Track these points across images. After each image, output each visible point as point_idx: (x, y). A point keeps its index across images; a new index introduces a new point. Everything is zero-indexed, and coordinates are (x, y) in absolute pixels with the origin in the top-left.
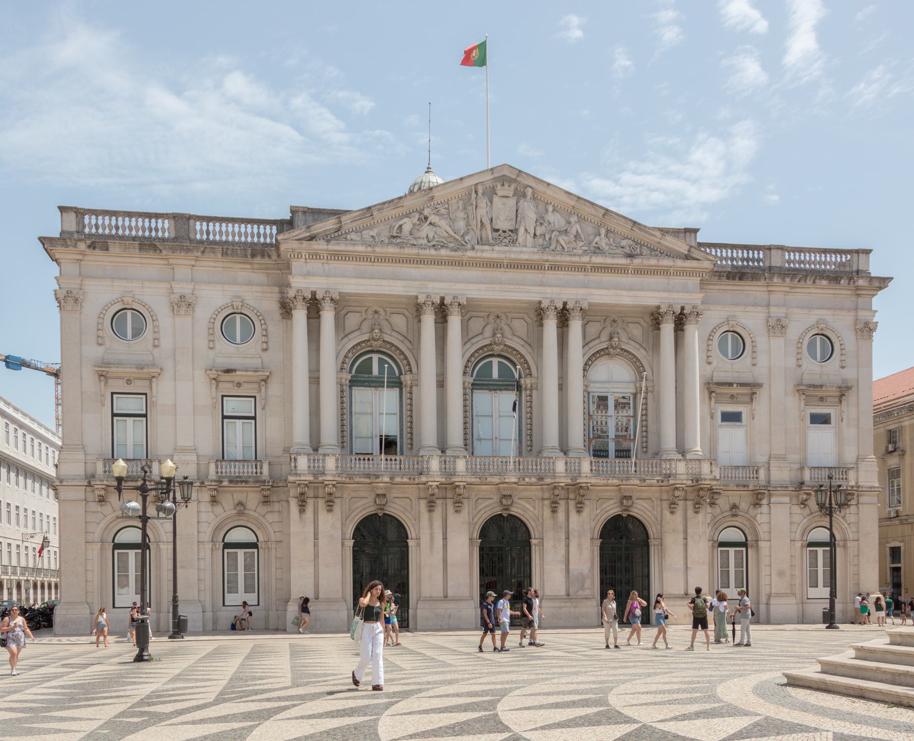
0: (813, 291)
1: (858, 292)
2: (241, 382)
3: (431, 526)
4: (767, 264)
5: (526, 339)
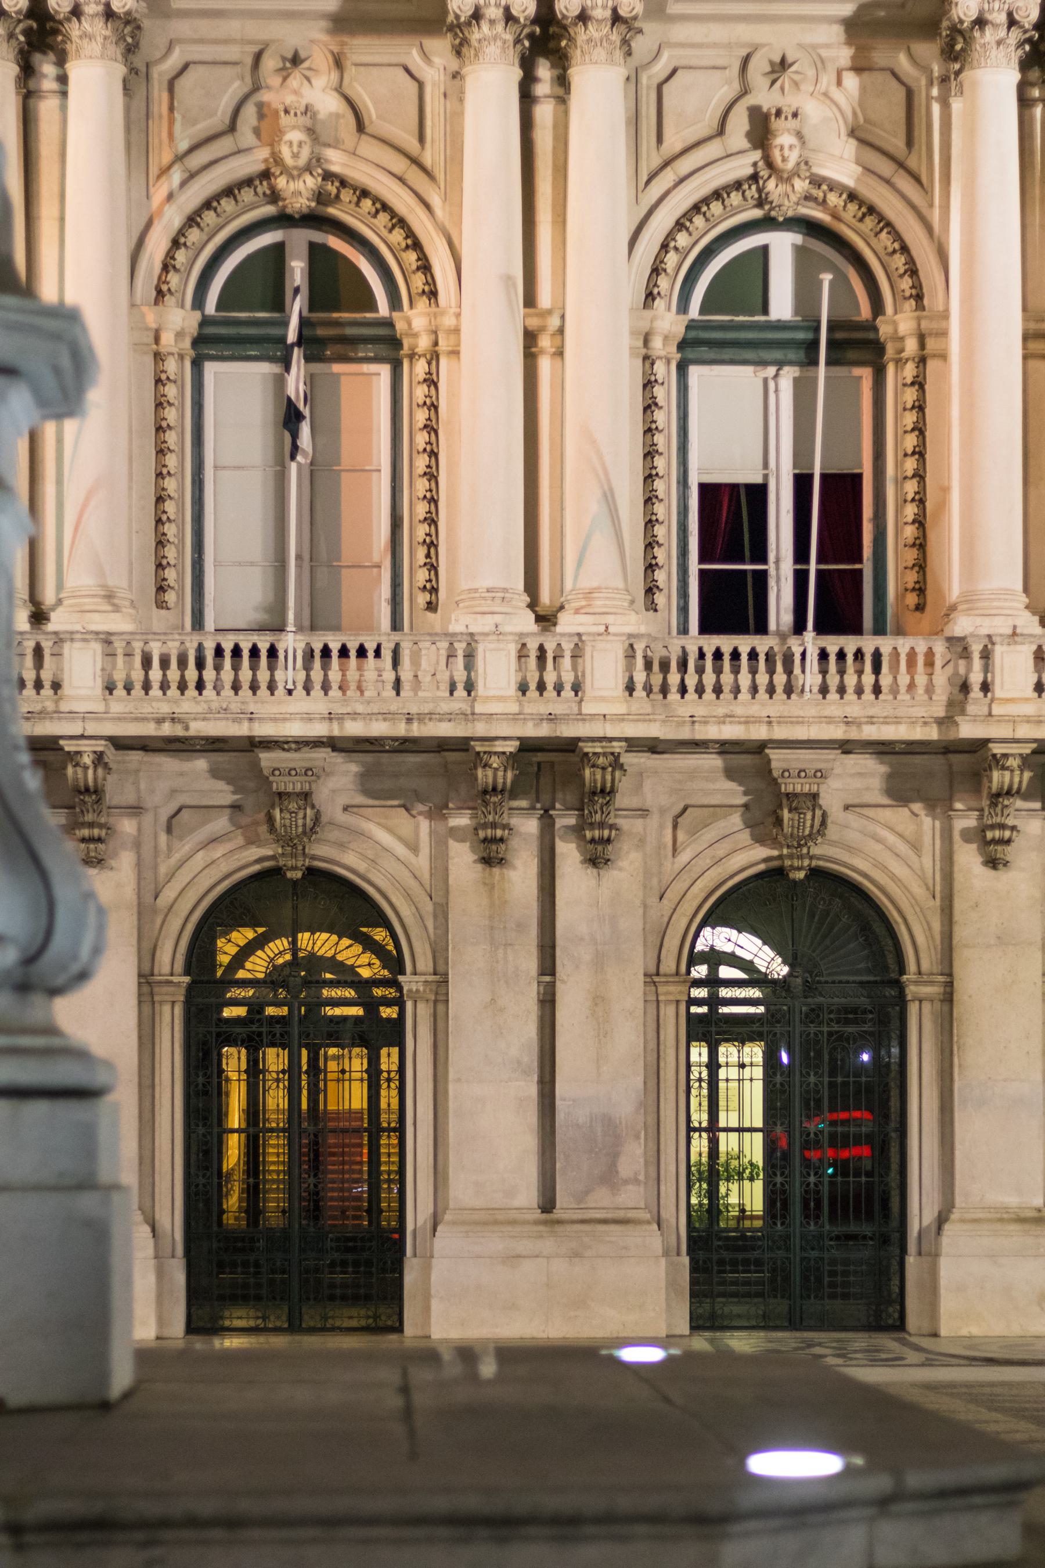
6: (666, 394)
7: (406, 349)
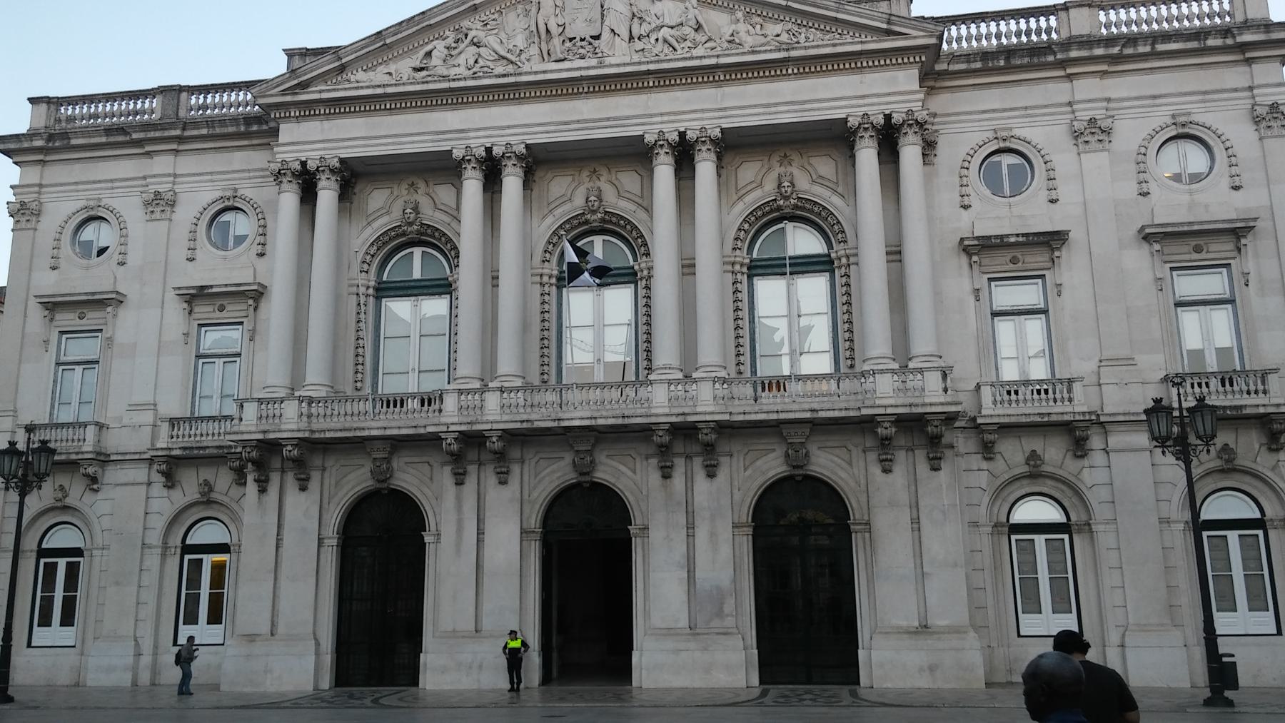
1: (1248, 55)
4: (1064, 34)
5: (640, 201)
6: (744, 287)
7: (639, 277)
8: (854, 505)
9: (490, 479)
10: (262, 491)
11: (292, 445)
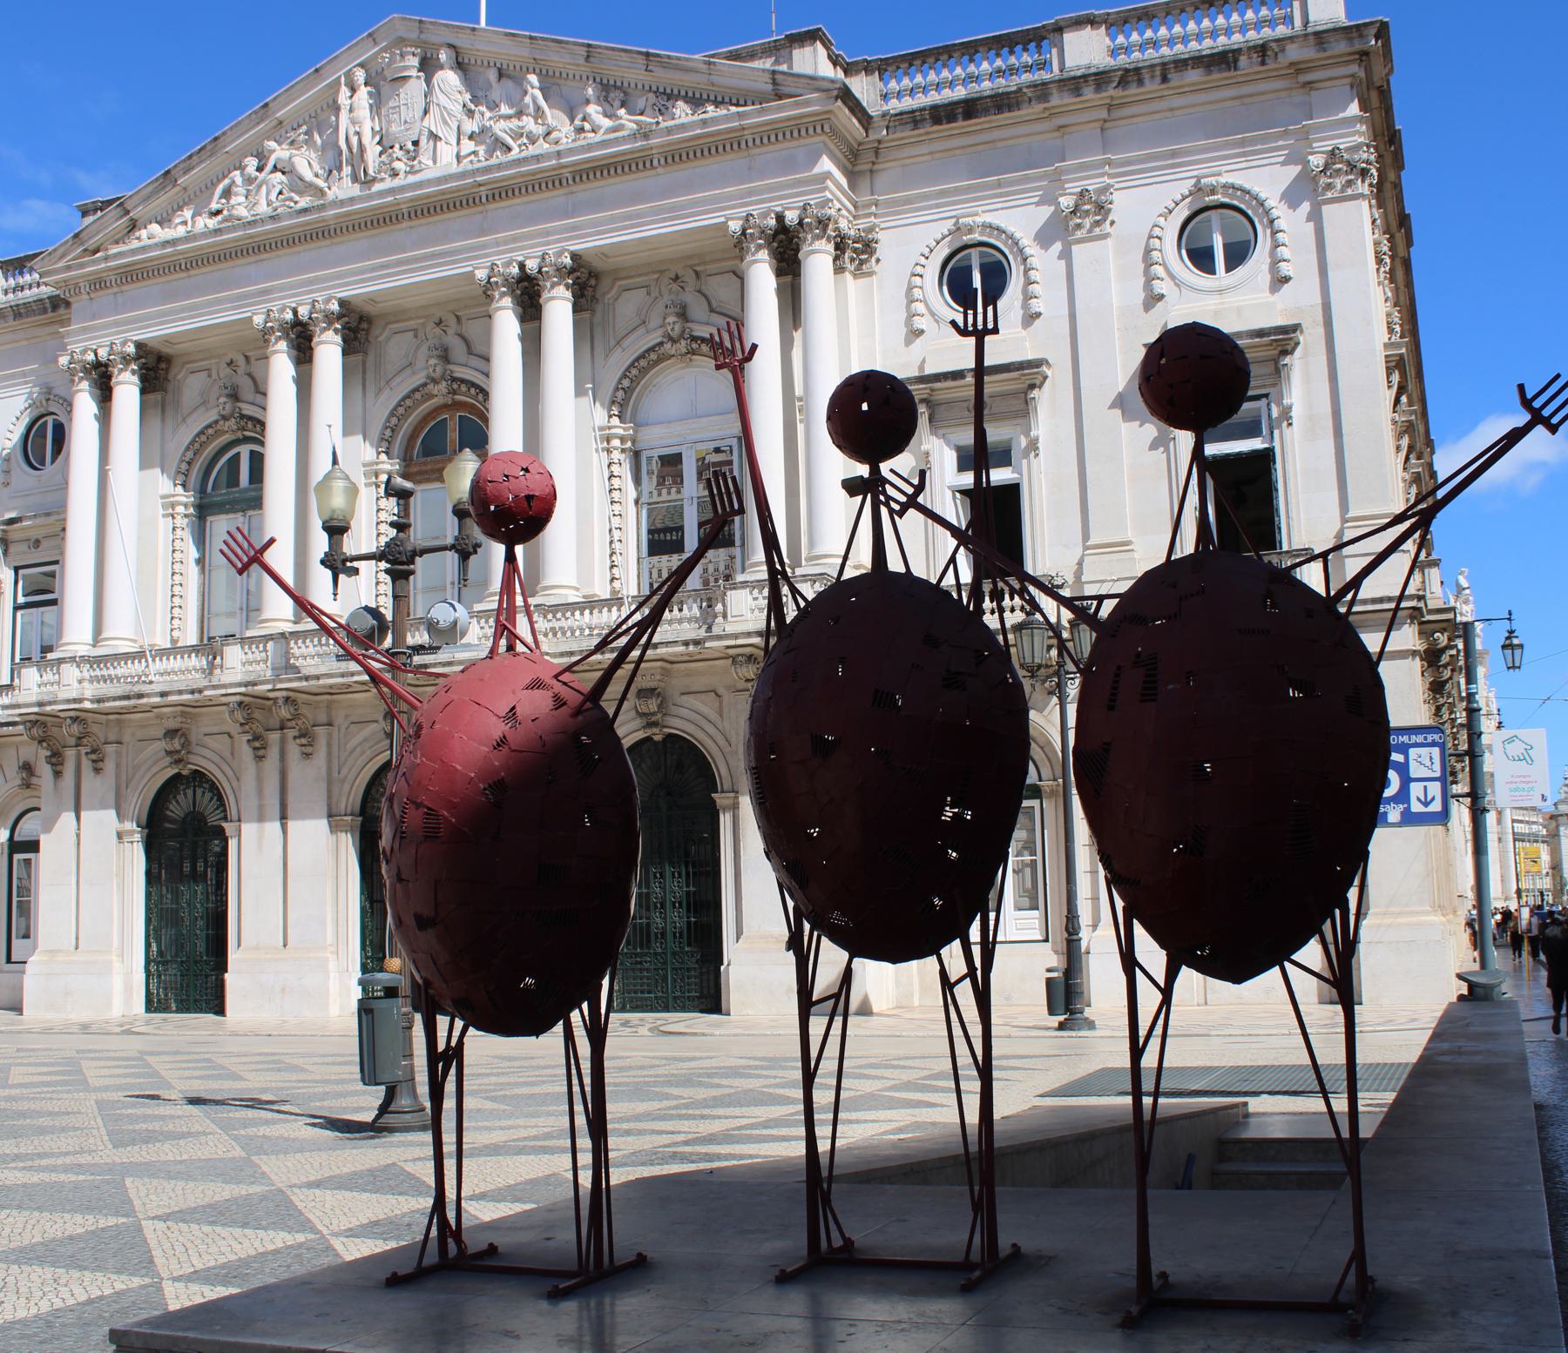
0: (1177, 102)
1: (1303, 78)
2: (40, 537)
3: (260, 792)
8: (724, 771)
9: (294, 750)
10: (58, 774)
11: (71, 718)
